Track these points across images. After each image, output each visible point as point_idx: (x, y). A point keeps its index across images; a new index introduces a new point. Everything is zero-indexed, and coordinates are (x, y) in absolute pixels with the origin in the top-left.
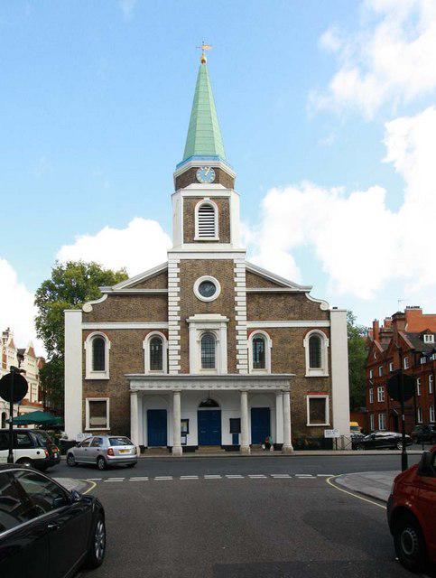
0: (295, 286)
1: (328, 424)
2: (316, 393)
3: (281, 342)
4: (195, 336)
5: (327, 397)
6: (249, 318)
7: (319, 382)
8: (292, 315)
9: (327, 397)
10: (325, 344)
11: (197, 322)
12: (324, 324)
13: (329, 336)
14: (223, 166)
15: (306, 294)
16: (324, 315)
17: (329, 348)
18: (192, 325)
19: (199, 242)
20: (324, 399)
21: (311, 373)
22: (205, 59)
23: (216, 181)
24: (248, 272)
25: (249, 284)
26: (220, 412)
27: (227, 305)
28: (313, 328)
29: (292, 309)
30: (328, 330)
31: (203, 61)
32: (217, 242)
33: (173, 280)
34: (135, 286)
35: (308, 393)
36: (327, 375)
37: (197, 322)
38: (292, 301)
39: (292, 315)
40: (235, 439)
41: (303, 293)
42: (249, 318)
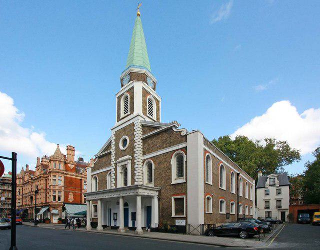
0: (165, 125)
1: (185, 216)
2: (178, 194)
3: (159, 164)
4: (119, 170)
5: (185, 197)
6: (144, 154)
7: (180, 187)
8: (165, 145)
9: (185, 197)
10: (185, 159)
11: (119, 162)
12: (183, 145)
13: (186, 154)
14: (134, 70)
15: (174, 129)
16: (184, 139)
17: (186, 162)
18: (118, 164)
19: (122, 119)
20: (183, 198)
21: (175, 180)
22: (139, 13)
23: (131, 80)
24: (143, 126)
25: (144, 133)
26: (128, 209)
27: (131, 151)
28: (175, 151)
29: (164, 142)
30: (185, 149)
31: (138, 15)
32: (129, 115)
33: (113, 143)
34: (104, 150)
35: (173, 195)
36: (185, 181)
37: (119, 162)
38: (165, 136)
39: (165, 145)
40: (134, 224)
41: (171, 128)
42: (144, 154)
